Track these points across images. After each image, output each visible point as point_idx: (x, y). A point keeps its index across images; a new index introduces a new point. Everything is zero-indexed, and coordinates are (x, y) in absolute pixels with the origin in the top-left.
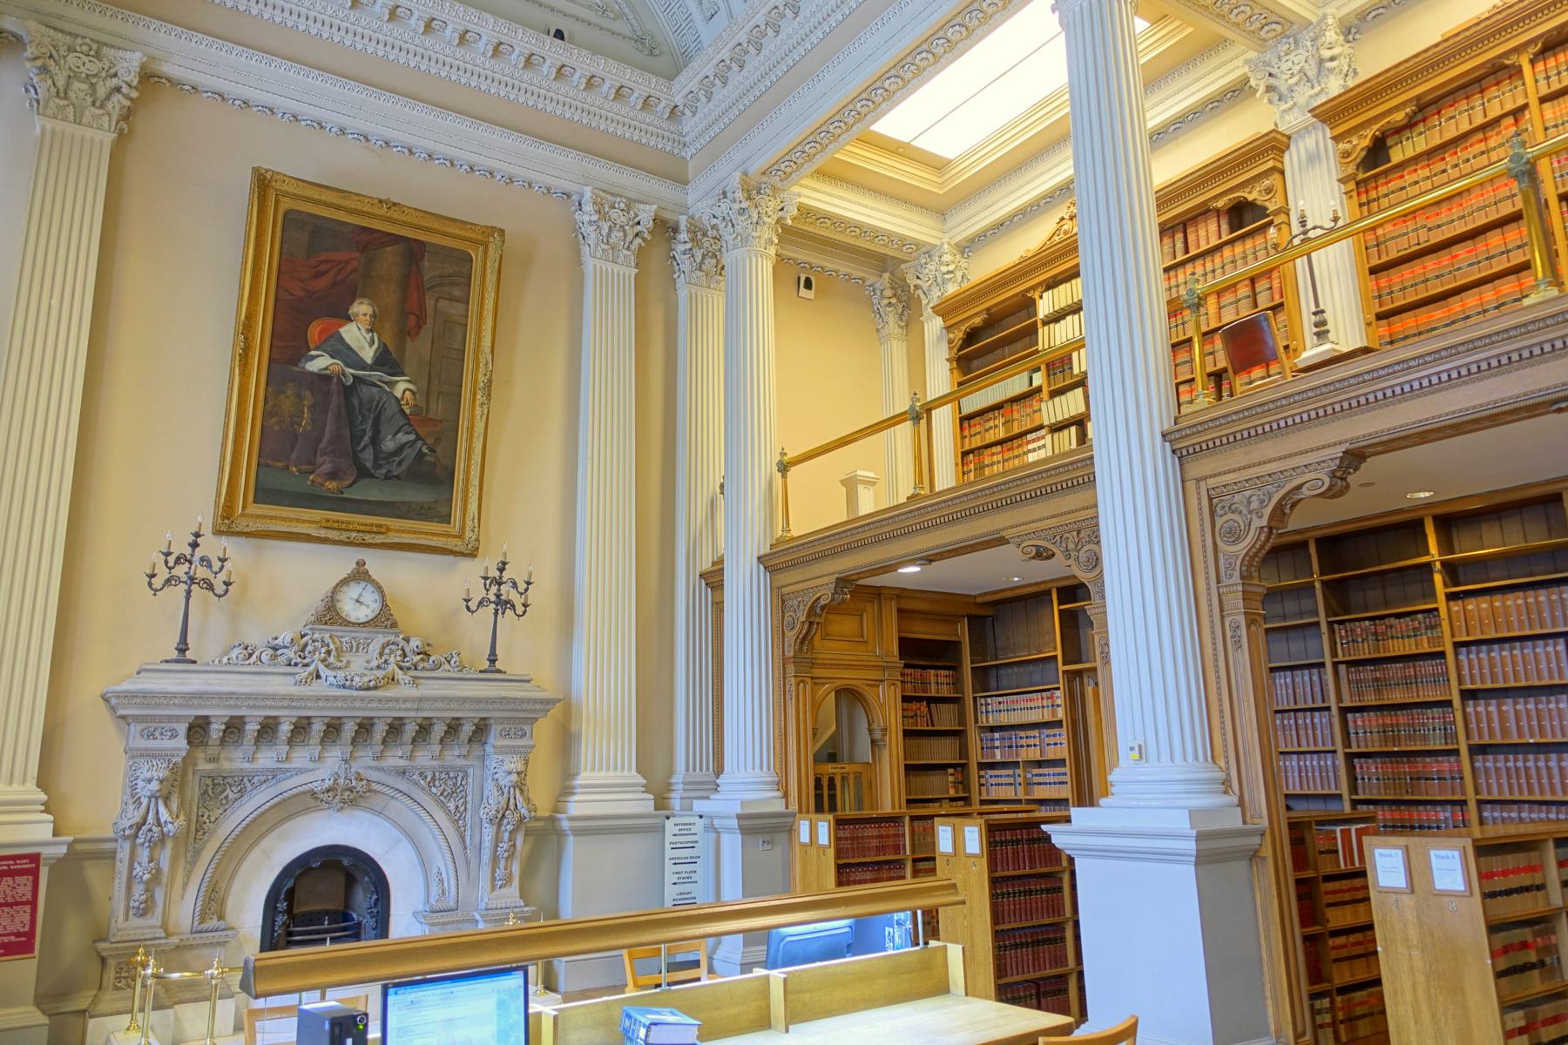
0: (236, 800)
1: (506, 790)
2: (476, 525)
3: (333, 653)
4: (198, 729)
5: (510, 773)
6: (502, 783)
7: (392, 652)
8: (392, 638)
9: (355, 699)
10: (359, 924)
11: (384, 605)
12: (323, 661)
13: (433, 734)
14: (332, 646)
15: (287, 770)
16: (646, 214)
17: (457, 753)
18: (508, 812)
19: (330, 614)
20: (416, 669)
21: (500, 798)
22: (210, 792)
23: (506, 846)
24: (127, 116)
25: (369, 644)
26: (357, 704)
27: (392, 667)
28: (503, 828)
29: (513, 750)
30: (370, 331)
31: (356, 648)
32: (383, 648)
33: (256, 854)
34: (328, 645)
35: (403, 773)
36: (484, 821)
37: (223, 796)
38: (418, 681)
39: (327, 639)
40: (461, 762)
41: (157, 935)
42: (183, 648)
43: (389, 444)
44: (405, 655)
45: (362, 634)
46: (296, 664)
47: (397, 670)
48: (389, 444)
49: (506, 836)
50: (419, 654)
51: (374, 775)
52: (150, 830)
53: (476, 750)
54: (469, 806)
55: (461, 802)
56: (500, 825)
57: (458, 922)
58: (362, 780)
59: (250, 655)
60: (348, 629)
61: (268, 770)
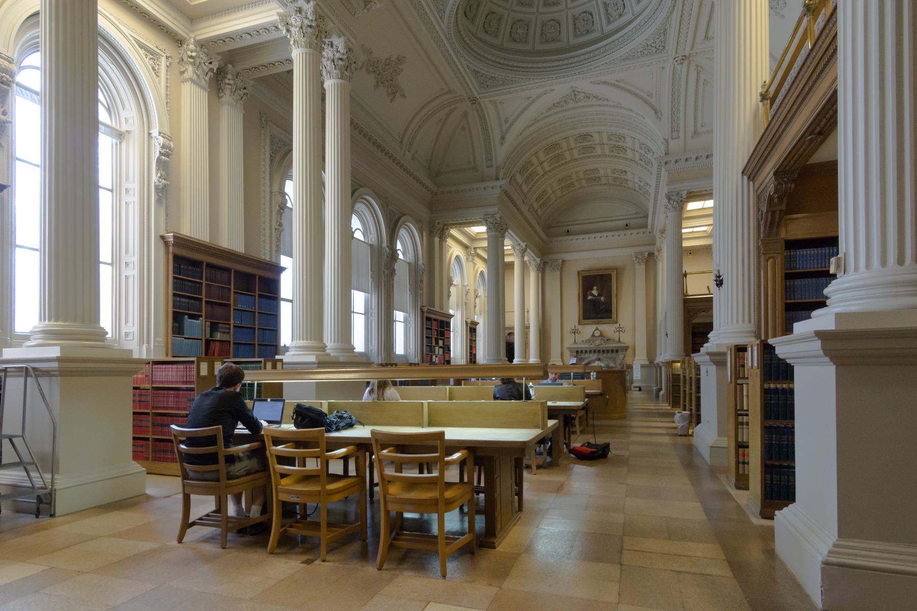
19: (593, 335)
43: (601, 308)
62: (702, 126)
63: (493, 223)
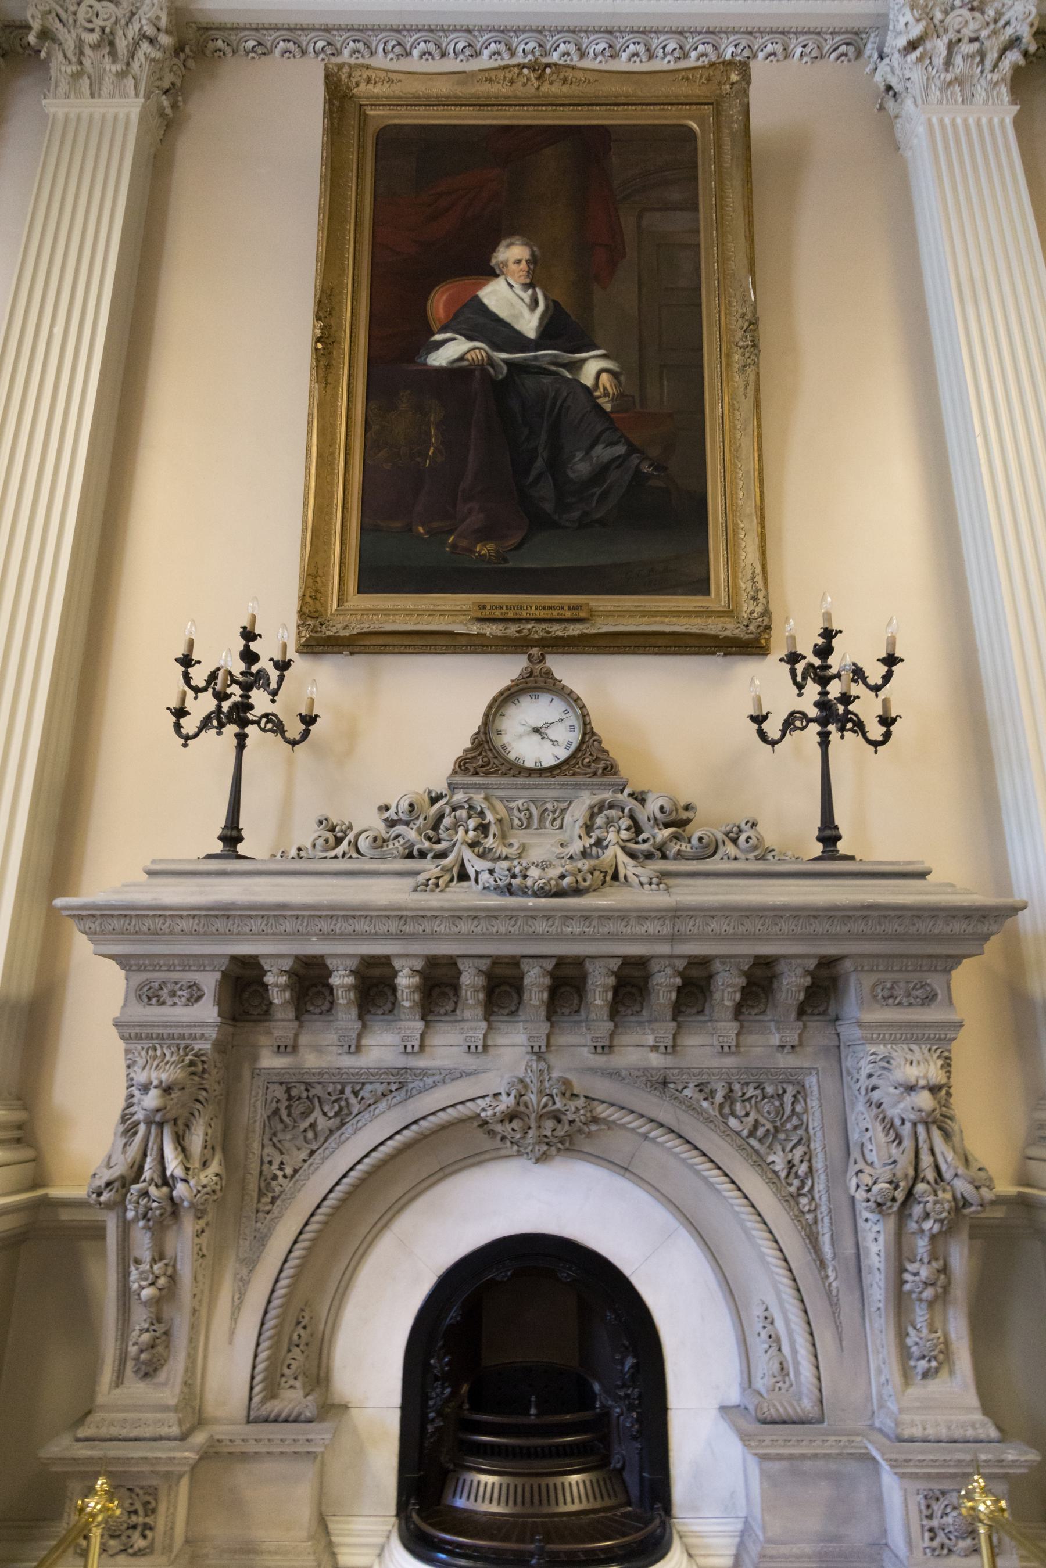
0: (331, 1132)
1: (906, 1130)
2: (760, 585)
3: (493, 829)
5: (911, 1088)
6: (894, 1112)
7: (609, 822)
8: (608, 795)
9: (532, 915)
10: (606, 1414)
11: (588, 734)
12: (472, 845)
13: (717, 996)
14: (490, 817)
15: (424, 1073)
17: (775, 1040)
18: (921, 1187)
20: (664, 857)
21: (894, 1150)
22: (284, 1113)
23: (924, 1273)
25: (563, 811)
26: (540, 927)
27: (613, 854)
28: (913, 1226)
30: (527, 286)
32: (592, 816)
33: (385, 1247)
34: (482, 814)
35: (662, 1083)
36: (861, 1206)
37: (305, 1124)
38: (671, 882)
39: (478, 799)
40: (786, 1061)
41: (164, 1431)
42: (232, 836)
43: (581, 467)
44: (637, 828)
45: (549, 792)
46: (422, 855)
47: (622, 858)
48: (581, 467)
49: (922, 1245)
50: (667, 825)
51: (602, 1088)
52: (145, 1194)
53: (818, 1034)
54: (819, 1164)
55: (799, 1152)
56: (903, 1214)
57: (827, 1456)
58: (574, 1096)
59: (339, 841)
60: (520, 780)
61: (389, 1071)
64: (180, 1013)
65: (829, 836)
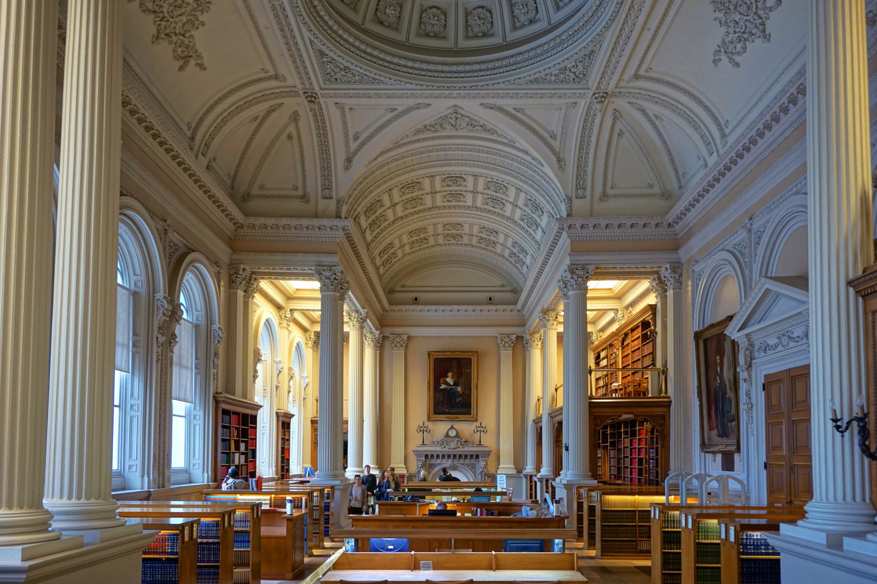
4: (426, 456)
16: (514, 337)
19: (447, 435)
24: (406, 346)
29: (484, 461)
31: (452, 441)
35: (463, 464)
42: (423, 442)
43: (458, 400)
45: (453, 439)
53: (477, 460)
62: (612, 188)
63: (330, 279)
64: (421, 459)
65: (480, 442)
